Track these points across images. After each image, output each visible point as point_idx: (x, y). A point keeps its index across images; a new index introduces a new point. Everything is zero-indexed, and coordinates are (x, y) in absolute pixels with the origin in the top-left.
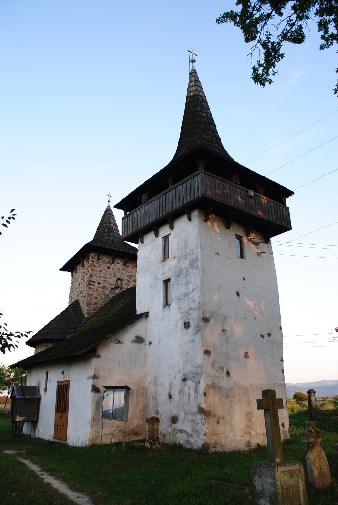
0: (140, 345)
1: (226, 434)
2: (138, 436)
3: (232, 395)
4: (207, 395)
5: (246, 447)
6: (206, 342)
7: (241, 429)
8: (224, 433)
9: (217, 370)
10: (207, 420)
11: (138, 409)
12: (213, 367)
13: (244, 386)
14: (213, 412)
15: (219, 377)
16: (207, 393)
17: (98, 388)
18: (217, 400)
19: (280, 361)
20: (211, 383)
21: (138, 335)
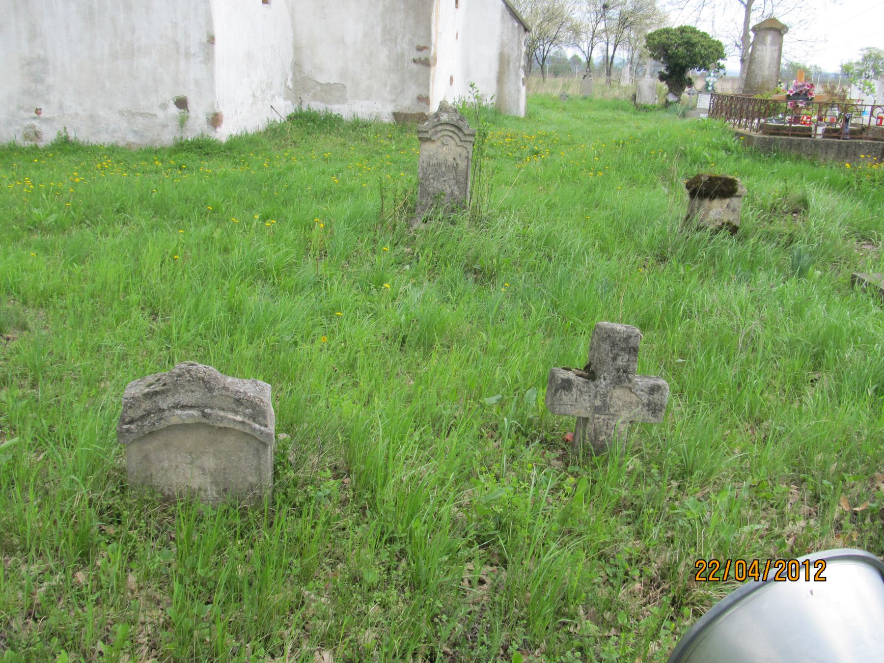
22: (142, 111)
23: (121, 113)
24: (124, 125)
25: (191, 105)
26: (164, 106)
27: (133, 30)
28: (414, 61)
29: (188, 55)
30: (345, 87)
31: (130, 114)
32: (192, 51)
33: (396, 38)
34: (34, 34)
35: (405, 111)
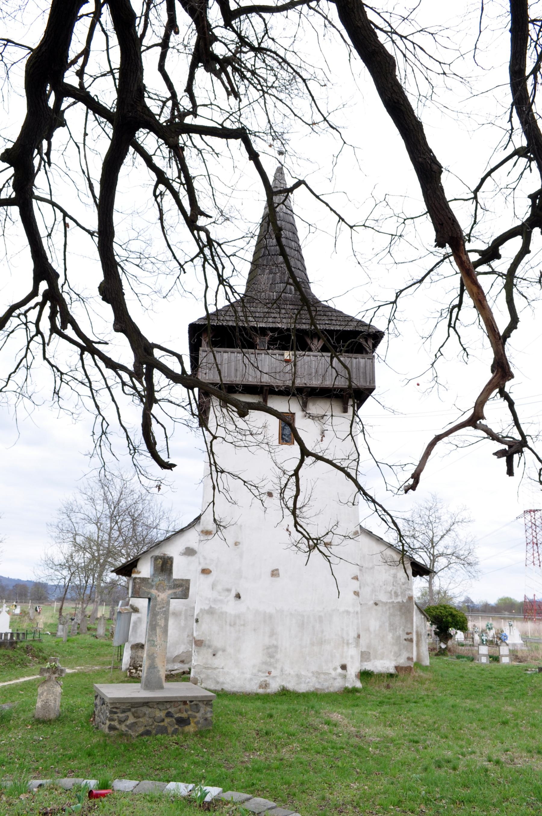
0: (191, 558)
1: (226, 670)
2: (185, 664)
3: (242, 623)
4: (199, 622)
5: (260, 688)
6: (205, 559)
7: (254, 666)
8: (223, 668)
9: (219, 592)
10: (197, 652)
11: (186, 633)
12: (213, 588)
13: (265, 612)
14: (207, 642)
15: (221, 601)
16: (199, 620)
17: (136, 608)
18: (216, 628)
19: (350, 578)
20: (207, 608)
21: (188, 546)
22: (324, 672)
23: (313, 673)
24: (314, 679)
25: (348, 668)
26: (335, 669)
27: (322, 632)
28: (405, 640)
29: (348, 644)
30: (370, 653)
31: (317, 674)
32: (350, 641)
33: (396, 628)
34: (273, 634)
35: (401, 665)
